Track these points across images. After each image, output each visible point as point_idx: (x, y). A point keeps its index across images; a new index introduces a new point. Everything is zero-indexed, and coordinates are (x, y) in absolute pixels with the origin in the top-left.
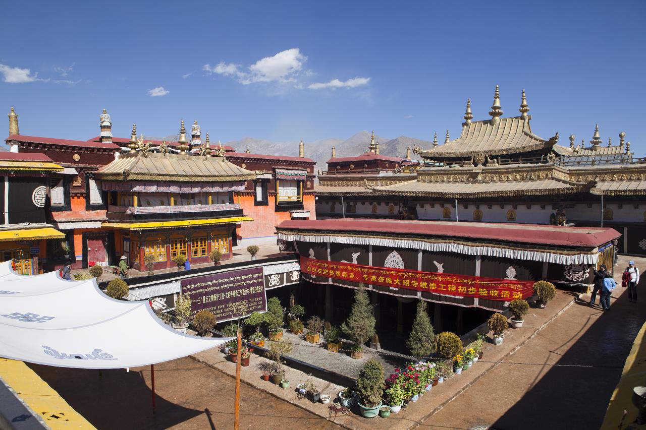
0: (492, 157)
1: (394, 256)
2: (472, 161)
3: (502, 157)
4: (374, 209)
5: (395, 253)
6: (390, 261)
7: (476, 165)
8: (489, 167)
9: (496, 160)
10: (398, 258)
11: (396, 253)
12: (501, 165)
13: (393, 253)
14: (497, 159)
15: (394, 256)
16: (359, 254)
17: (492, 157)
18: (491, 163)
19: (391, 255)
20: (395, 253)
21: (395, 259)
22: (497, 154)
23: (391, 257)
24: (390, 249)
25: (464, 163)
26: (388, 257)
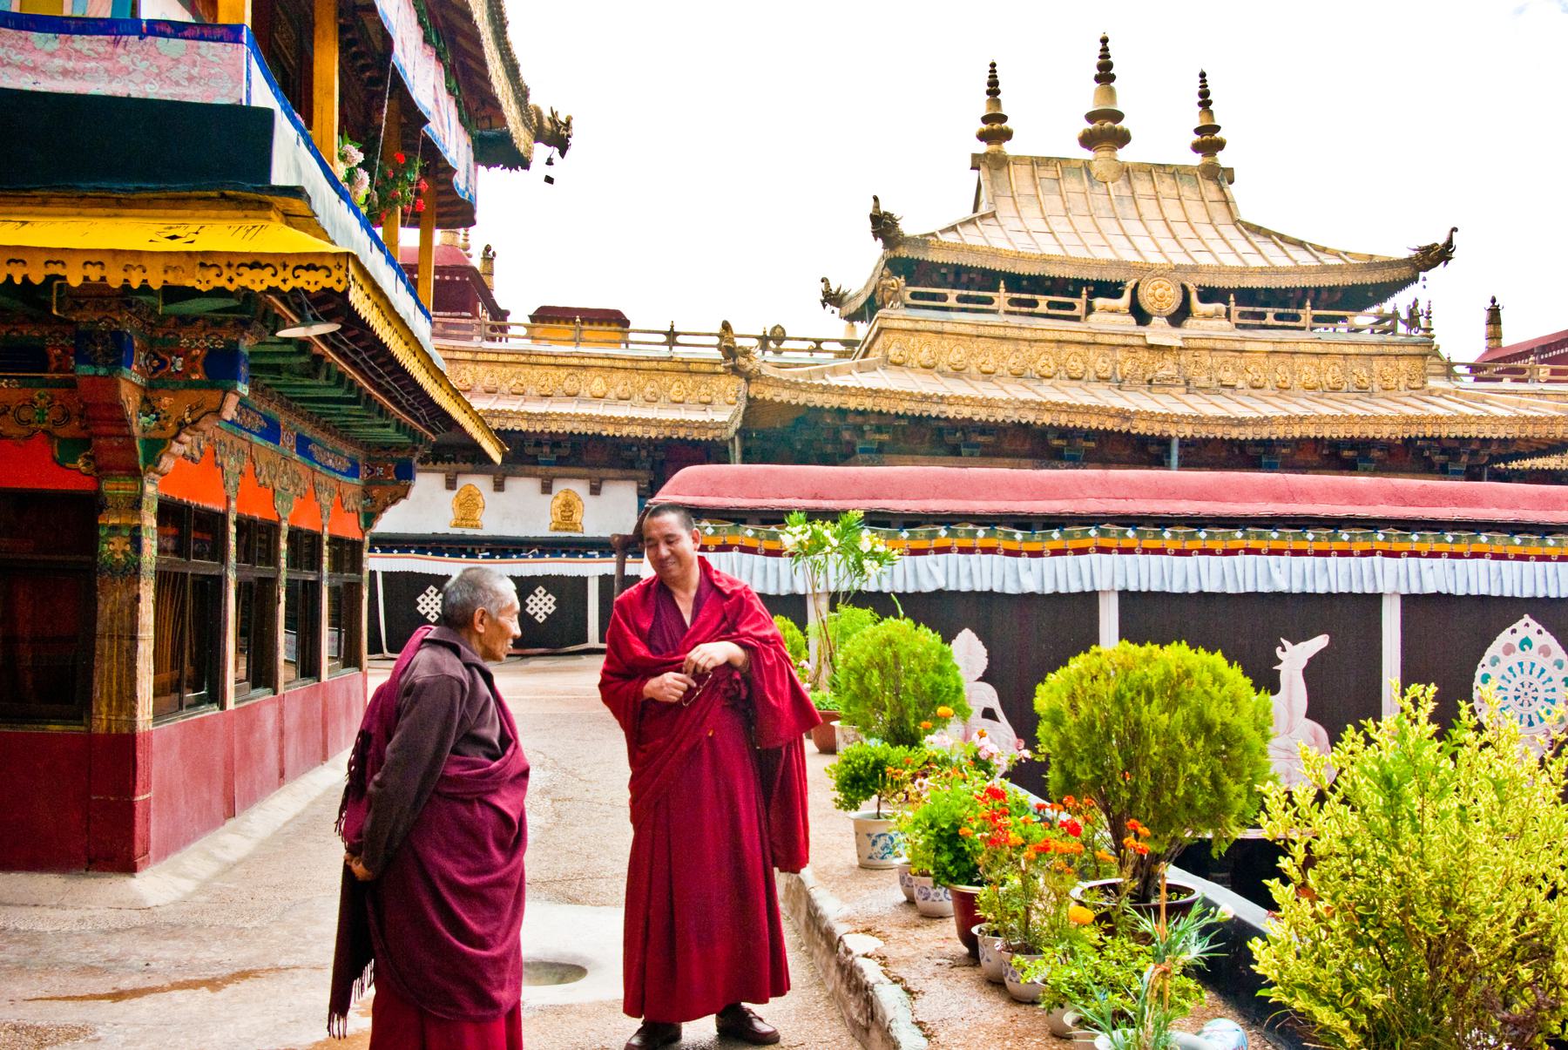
0: (1209, 295)
1: (1526, 642)
2: (1124, 301)
3: (1247, 296)
4: (468, 507)
5: (1527, 627)
6: (1502, 668)
7: (1140, 315)
8: (1192, 327)
9: (1221, 307)
10: (1545, 651)
11: (1535, 626)
12: (1237, 325)
13: (1519, 625)
14: (1227, 302)
15: (1526, 642)
16: (1321, 642)
17: (1208, 295)
18: (1206, 317)
19: (1505, 637)
20: (1527, 627)
21: (1532, 655)
22: (1219, 282)
23: (1509, 650)
24: (1494, 613)
25: (1090, 309)
26: (1495, 649)
